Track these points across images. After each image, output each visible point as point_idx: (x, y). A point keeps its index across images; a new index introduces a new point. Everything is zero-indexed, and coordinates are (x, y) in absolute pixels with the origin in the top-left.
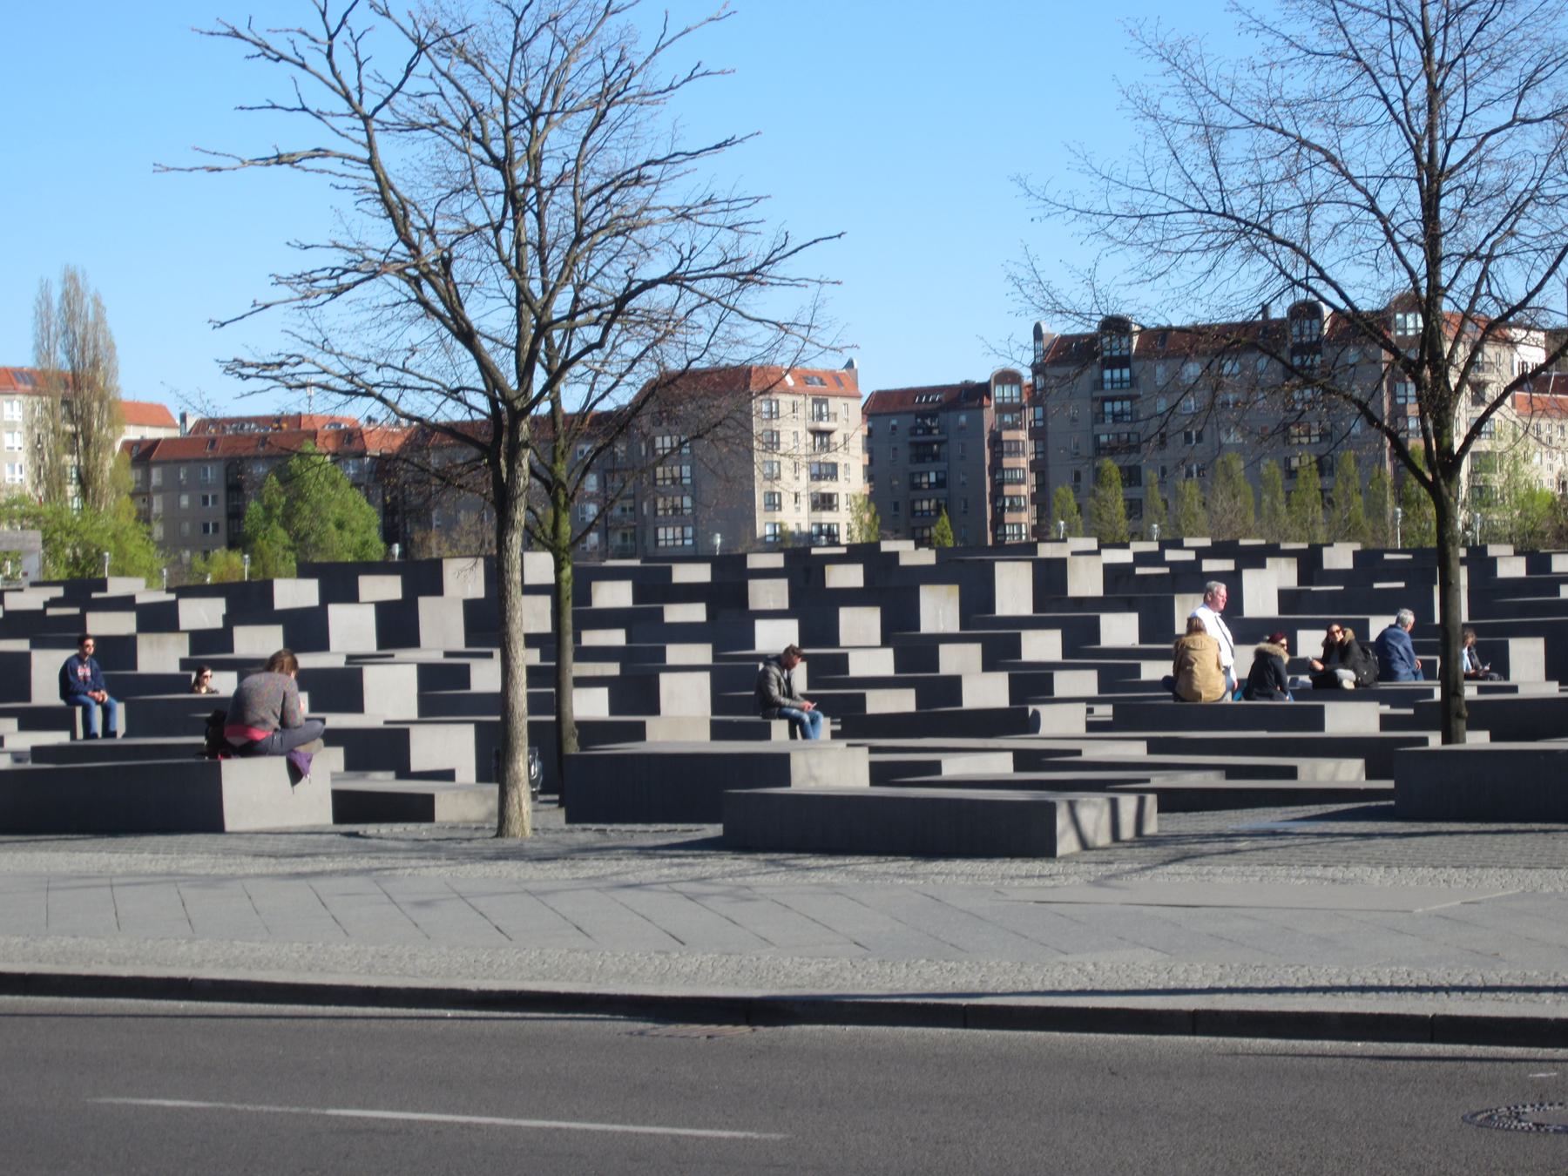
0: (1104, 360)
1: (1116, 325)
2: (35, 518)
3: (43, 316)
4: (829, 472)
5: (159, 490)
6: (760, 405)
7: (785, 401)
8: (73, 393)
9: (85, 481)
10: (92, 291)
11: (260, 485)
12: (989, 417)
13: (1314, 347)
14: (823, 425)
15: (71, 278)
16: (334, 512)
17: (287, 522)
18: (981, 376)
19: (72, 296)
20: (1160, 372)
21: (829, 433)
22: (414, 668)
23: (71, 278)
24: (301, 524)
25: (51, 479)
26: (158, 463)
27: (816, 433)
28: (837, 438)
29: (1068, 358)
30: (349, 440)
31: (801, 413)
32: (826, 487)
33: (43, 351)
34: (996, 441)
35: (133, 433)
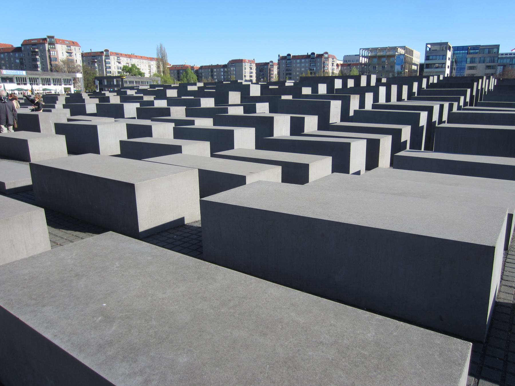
2: (158, 76)
3: (158, 50)
4: (251, 73)
6: (244, 64)
7: (247, 64)
8: (161, 60)
9: (164, 72)
11: (182, 73)
12: (269, 67)
13: (313, 58)
15: (161, 45)
16: (192, 76)
17: (186, 77)
18: (268, 62)
19: (161, 48)
23: (161, 45)
24: (188, 78)
25: (159, 71)
29: (282, 59)
30: (192, 68)
33: (158, 55)
34: (270, 69)
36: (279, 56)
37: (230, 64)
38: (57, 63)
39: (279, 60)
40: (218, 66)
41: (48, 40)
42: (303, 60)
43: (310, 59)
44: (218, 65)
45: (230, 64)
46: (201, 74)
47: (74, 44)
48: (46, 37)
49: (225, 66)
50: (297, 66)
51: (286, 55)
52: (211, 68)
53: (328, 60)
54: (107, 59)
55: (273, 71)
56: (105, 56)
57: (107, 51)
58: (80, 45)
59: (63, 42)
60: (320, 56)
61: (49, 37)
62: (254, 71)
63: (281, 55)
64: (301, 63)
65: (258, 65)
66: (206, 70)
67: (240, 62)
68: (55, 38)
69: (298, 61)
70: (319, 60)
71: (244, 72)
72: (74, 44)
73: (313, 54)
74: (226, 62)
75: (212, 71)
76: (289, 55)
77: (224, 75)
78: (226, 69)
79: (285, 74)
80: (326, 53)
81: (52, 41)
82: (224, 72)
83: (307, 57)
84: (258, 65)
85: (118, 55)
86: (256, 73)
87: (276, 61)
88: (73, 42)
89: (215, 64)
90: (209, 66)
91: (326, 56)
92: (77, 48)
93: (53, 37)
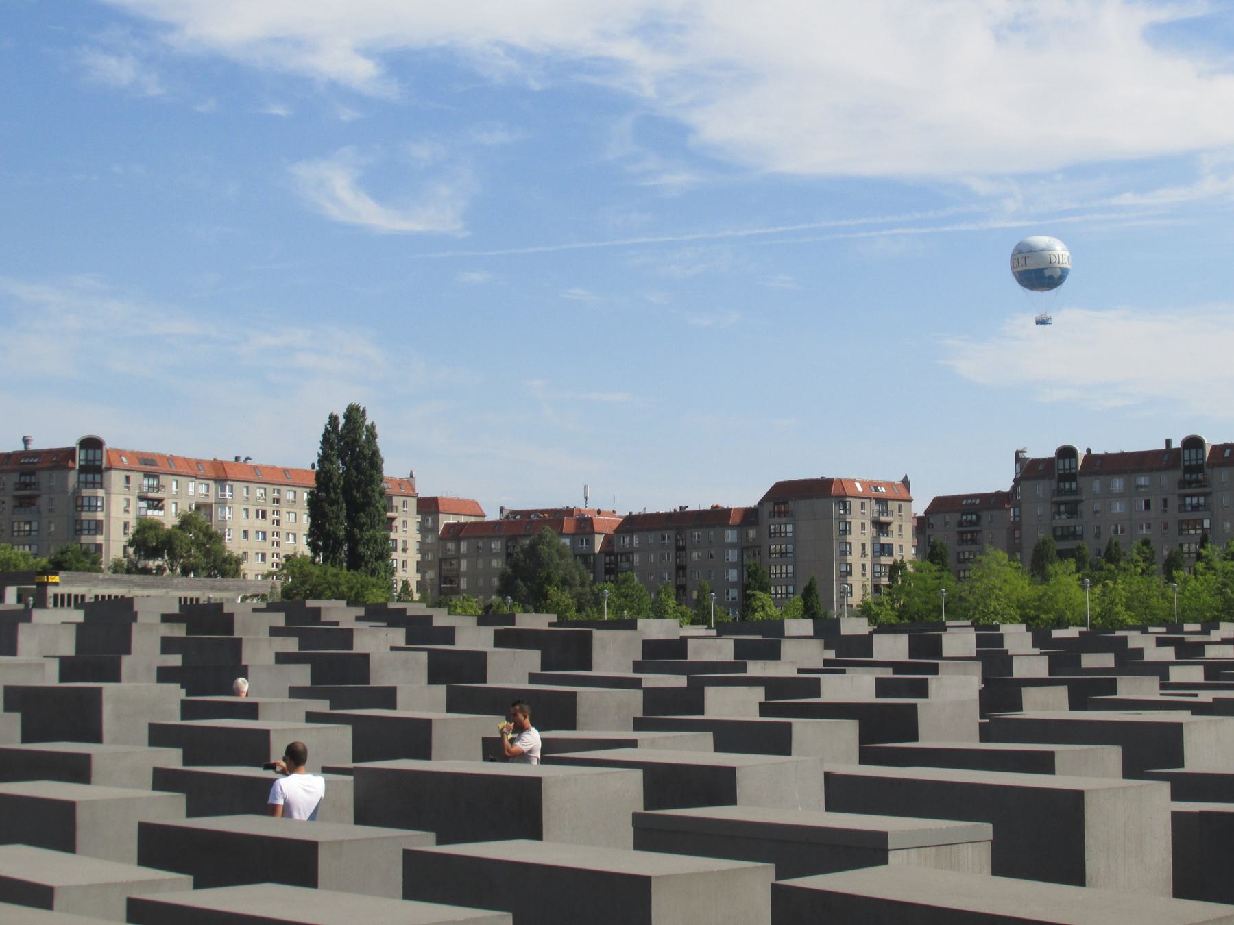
0: (1060, 475)
1: (1067, 453)
5: (465, 556)
10: (368, 423)
13: (1198, 468)
14: (883, 519)
20: (1097, 485)
21: (888, 524)
26: (464, 538)
28: (894, 528)
31: (867, 511)
35: (452, 520)
37: (769, 507)
40: (717, 517)
42: (1142, 480)
43: (1178, 474)
44: (715, 509)
45: (769, 507)
46: (627, 555)
49: (750, 516)
50: (1113, 506)
51: (1051, 454)
52: (681, 521)
54: (87, 484)
56: (83, 470)
57: (92, 444)
63: (1033, 454)
66: (653, 538)
69: (1118, 484)
73: (1194, 443)
74: (744, 494)
76: (1067, 453)
77: (740, 565)
78: (752, 533)
82: (744, 548)
85: (151, 467)
89: (699, 502)
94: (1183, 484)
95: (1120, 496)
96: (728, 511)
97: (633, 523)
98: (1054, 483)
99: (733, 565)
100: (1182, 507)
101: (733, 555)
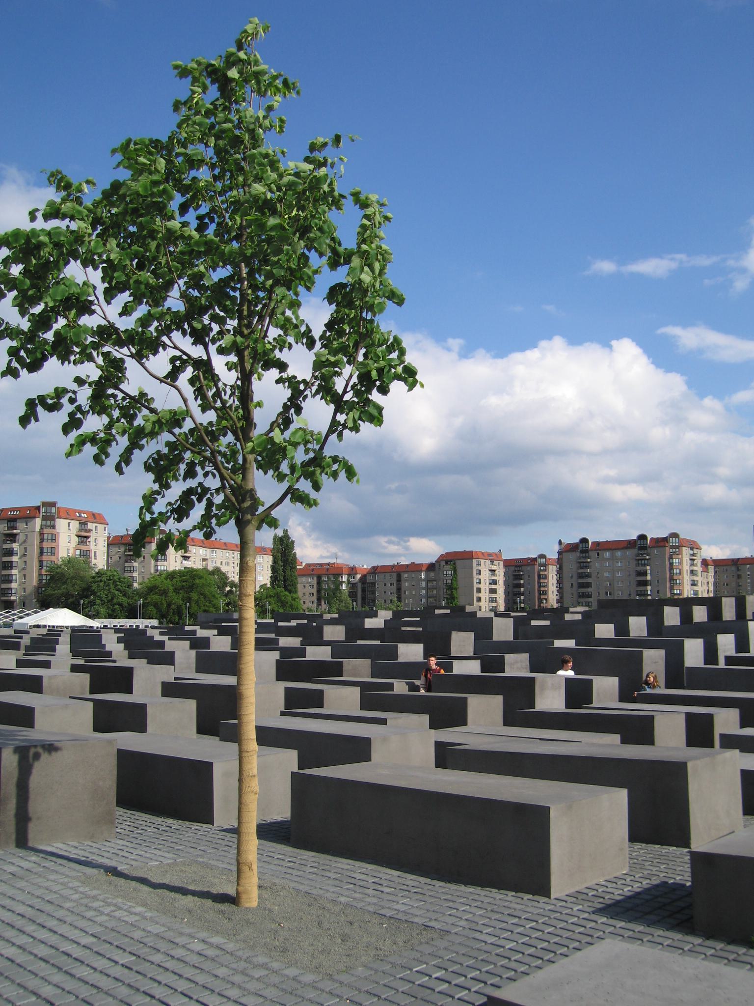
4: (494, 582)
22: (683, 716)
27: (491, 570)
29: (566, 550)
32: (493, 587)
36: (560, 542)
38: (53, 558)
39: (560, 553)
40: (414, 568)
41: (43, 510)
42: (619, 553)
43: (635, 551)
46: (374, 584)
47: (97, 518)
48: (38, 503)
49: (431, 567)
53: (680, 553)
55: (546, 577)
58: (108, 519)
59: (69, 514)
60: (661, 542)
61: (45, 504)
62: (500, 577)
63: (566, 541)
64: (613, 558)
65: (508, 564)
67: (468, 556)
68: (58, 505)
69: (607, 554)
70: (655, 551)
71: (475, 581)
72: (97, 518)
75: (399, 580)
78: (432, 574)
79: (575, 585)
80: (675, 535)
81: (48, 513)
82: (428, 581)
83: (630, 544)
84: (508, 564)
86: (506, 583)
87: (553, 555)
88: (93, 514)
90: (393, 566)
91: (673, 541)
92: (100, 527)
93: (53, 504)
94: (638, 555)
95: (608, 559)
96: (421, 565)
97: (375, 570)
98: (578, 554)
99: (423, 589)
100: (638, 565)
101: (424, 584)
